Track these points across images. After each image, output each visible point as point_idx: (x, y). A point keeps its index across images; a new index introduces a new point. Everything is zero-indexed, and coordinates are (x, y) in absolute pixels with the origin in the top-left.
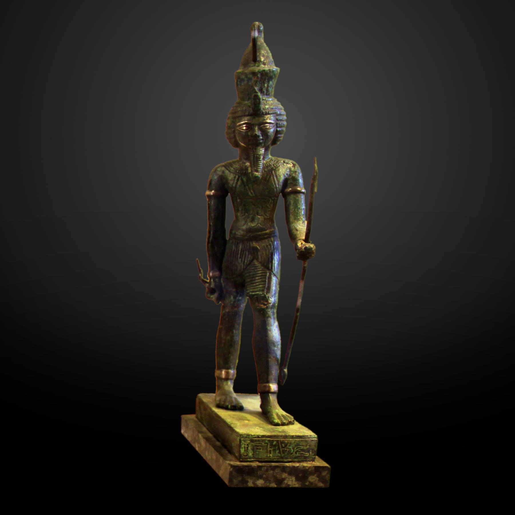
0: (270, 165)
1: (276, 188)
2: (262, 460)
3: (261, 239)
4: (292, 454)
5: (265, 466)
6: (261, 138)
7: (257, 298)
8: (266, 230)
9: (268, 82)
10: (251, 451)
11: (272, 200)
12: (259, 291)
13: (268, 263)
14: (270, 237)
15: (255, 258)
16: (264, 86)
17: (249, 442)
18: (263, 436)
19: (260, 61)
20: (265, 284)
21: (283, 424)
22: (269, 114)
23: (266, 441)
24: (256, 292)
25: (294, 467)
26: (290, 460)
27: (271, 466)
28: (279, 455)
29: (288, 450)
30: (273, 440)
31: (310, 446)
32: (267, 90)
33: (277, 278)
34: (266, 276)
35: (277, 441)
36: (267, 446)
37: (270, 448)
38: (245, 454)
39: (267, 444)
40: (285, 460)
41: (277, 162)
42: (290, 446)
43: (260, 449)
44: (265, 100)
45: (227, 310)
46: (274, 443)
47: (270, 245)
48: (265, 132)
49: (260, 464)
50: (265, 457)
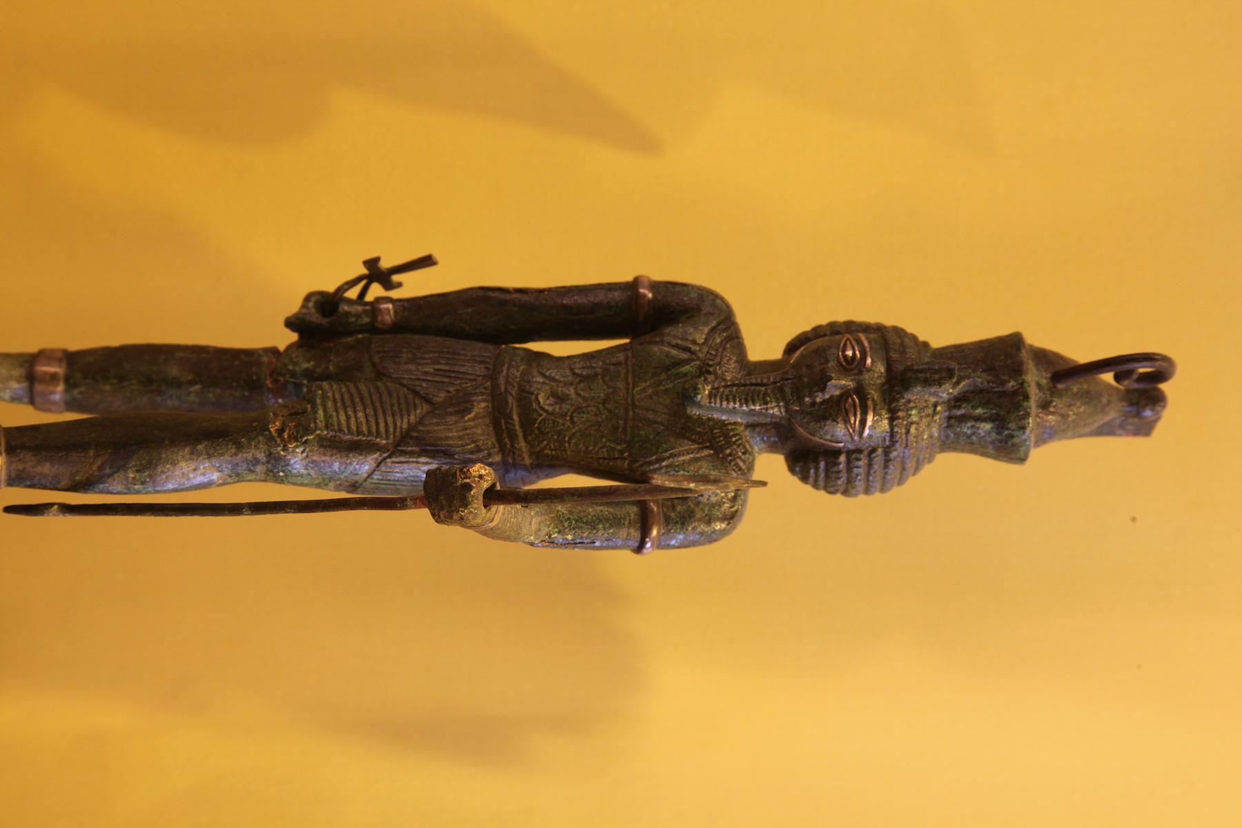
1: (659, 460)
3: (496, 425)
6: (818, 400)
7: (305, 411)
8: (526, 440)
9: (991, 419)
11: (622, 452)
12: (327, 416)
13: (419, 441)
14: (502, 450)
15: (437, 409)
16: (974, 408)
19: (1053, 391)
20: (350, 432)
22: (892, 420)
24: (324, 406)
32: (962, 419)
33: (370, 475)
34: (378, 434)
41: (740, 469)
44: (935, 413)
45: (265, 359)
47: (479, 450)
48: (836, 409)
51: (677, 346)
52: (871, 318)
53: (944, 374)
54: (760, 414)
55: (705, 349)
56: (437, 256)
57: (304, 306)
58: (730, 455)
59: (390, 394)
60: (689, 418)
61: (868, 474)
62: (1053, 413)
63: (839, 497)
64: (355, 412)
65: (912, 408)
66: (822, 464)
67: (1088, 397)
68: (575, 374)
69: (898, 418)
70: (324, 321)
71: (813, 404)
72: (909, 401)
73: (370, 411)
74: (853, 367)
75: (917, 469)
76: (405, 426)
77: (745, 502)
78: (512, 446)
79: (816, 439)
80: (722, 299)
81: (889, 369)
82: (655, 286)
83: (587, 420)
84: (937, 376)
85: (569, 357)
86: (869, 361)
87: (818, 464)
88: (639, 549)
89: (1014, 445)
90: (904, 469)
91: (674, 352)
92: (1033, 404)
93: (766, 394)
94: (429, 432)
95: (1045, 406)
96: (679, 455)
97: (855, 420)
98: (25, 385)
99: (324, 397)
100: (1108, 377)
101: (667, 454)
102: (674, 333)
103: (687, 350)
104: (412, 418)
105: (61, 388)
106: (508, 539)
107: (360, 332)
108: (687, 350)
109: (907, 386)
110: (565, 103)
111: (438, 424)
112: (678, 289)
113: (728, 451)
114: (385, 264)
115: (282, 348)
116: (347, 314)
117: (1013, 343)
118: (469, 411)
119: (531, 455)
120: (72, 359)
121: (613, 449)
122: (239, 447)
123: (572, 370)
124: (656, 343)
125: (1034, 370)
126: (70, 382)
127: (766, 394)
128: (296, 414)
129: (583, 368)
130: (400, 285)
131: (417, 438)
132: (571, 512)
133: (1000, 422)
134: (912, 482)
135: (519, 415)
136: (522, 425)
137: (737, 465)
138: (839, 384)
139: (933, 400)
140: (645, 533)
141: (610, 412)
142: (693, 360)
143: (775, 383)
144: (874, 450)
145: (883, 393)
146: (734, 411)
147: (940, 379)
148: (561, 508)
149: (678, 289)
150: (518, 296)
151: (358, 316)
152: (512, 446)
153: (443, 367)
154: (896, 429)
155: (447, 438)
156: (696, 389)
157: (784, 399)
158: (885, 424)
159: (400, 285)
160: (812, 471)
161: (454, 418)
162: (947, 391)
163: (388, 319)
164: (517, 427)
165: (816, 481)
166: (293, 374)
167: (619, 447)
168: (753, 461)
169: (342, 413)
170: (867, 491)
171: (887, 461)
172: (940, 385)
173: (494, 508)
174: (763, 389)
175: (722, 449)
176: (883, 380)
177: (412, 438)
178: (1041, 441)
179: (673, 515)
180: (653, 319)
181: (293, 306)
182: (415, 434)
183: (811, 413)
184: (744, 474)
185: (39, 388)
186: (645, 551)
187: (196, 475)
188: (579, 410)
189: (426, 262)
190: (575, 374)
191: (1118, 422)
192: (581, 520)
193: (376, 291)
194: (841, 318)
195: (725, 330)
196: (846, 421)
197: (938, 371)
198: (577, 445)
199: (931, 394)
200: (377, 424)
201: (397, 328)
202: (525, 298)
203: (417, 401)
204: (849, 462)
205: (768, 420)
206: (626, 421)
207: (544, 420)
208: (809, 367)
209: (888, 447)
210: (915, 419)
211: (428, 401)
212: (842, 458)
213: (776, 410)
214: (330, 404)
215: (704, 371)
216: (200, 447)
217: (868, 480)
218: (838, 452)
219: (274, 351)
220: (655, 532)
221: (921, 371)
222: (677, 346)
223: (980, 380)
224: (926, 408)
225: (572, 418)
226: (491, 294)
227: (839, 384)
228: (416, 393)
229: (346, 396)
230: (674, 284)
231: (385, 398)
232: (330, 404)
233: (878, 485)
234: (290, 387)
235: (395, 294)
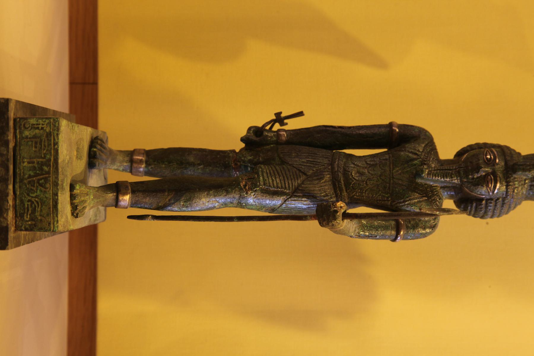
0: (433, 195)
1: (404, 202)
2: (18, 151)
3: (334, 185)
4: (28, 195)
5: (8, 152)
6: (475, 177)
10: (32, 134)
11: (388, 198)
17: (47, 130)
18: (57, 151)
20: (274, 187)
21: (73, 197)
22: (507, 186)
23: (48, 156)
24: (263, 175)
25: (7, 195)
26: (18, 193)
27: (8, 160)
28: (26, 176)
29: (35, 189)
30: (50, 165)
31: (41, 220)
34: (285, 188)
35: (48, 173)
36: (42, 158)
37: (38, 163)
38: (27, 126)
39: (45, 157)
40: (17, 186)
42: (41, 191)
43: (36, 147)
44: (525, 183)
46: (45, 168)
48: (483, 181)
49: (11, 145)
50: (22, 155)
51: (412, 152)
52: (495, 142)
53: (532, 167)
54: (449, 182)
55: (423, 154)
56: (304, 112)
58: (434, 200)
59: (289, 171)
60: (417, 183)
61: (494, 209)
64: (276, 178)
65: (516, 181)
66: (474, 205)
68: (367, 164)
69: (510, 185)
70: (257, 139)
71: (473, 178)
72: (515, 178)
73: (281, 178)
74: (490, 163)
75: (515, 208)
76: (296, 184)
77: (439, 220)
78: (341, 194)
79: (473, 194)
80: (428, 132)
82: (400, 126)
83: (373, 184)
84: (528, 168)
85: (363, 156)
86: (497, 161)
87: (473, 204)
88: (395, 240)
91: (410, 155)
93: (452, 174)
94: (306, 187)
96: (413, 199)
97: (491, 186)
98: (129, 164)
99: (262, 172)
101: (408, 199)
102: (409, 146)
103: (416, 154)
104: (299, 181)
107: (272, 144)
108: (416, 154)
109: (515, 171)
110: (346, 46)
111: (310, 184)
112: (409, 128)
113: (433, 198)
114: (283, 115)
115: (237, 151)
118: (322, 178)
119: (348, 198)
120: (148, 153)
121: (384, 196)
122: (228, 192)
123: (366, 162)
124: (403, 151)
126: (148, 164)
127: (452, 174)
128: (251, 178)
129: (371, 161)
130: (287, 124)
131: (302, 190)
132: (367, 224)
134: (512, 213)
135: (344, 181)
136: (345, 185)
137: (436, 204)
138: (485, 170)
139: (525, 178)
140: (398, 233)
141: (383, 180)
142: (418, 158)
143: (456, 169)
144: (498, 199)
147: (530, 168)
148: (364, 222)
149: (409, 128)
150: (340, 129)
151: (271, 137)
152: (341, 194)
153: (310, 160)
154: (509, 190)
155: (314, 190)
157: (460, 176)
159: (287, 124)
160: (469, 208)
161: (316, 182)
163: (284, 138)
164: (343, 186)
165: (470, 212)
166: (244, 162)
167: (387, 196)
169: (270, 179)
171: (503, 204)
172: (530, 171)
173: (345, 221)
174: (451, 171)
175: (430, 197)
177: (299, 190)
179: (409, 225)
180: (400, 141)
181: (244, 133)
182: (300, 188)
183: (472, 182)
185: (135, 165)
186: (397, 241)
187: (207, 203)
188: (369, 179)
189: (300, 114)
190: (367, 164)
192: (370, 227)
193: (277, 127)
194: (481, 141)
195: (431, 146)
196: (487, 186)
197: (529, 165)
198: (368, 194)
199: (524, 175)
200: (285, 184)
201: (288, 142)
203: (301, 174)
204: (486, 204)
205: (451, 185)
206: (390, 184)
207: (354, 183)
208: (471, 162)
209: (505, 198)
210: (517, 186)
211: (305, 174)
212: (484, 202)
213: (456, 181)
214: (265, 175)
216: (211, 192)
217: (494, 212)
218: (482, 200)
219: (234, 151)
220: (402, 233)
222: (412, 152)
224: (521, 182)
225: (366, 182)
226: (328, 128)
229: (271, 171)
230: (408, 126)
231: (288, 173)
232: (265, 175)
234: (242, 167)
235: (286, 128)
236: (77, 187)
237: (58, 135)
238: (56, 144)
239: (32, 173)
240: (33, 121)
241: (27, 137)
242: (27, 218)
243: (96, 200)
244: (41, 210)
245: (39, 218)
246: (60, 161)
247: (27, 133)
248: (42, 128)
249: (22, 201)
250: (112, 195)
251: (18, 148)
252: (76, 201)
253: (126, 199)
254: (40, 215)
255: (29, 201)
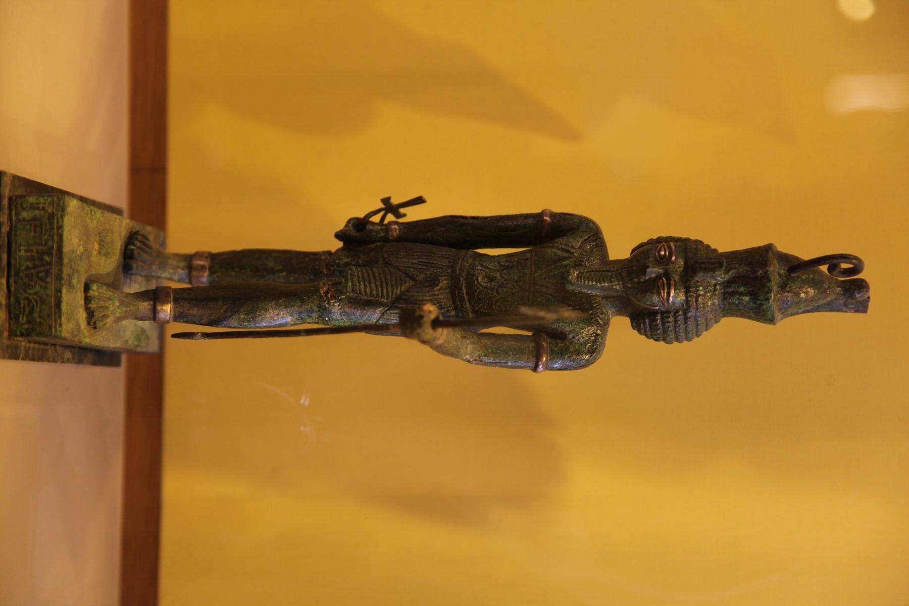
3: (453, 295)
6: (642, 280)
7: (341, 283)
14: (456, 309)
16: (739, 287)
18: (61, 237)
21: (88, 300)
22: (686, 293)
26: (13, 289)
28: (23, 268)
29: (32, 283)
32: (732, 294)
35: (50, 264)
37: (37, 252)
40: (12, 281)
42: (41, 286)
43: (35, 232)
44: (715, 290)
46: (47, 258)
48: (653, 286)
51: (562, 249)
54: (609, 289)
56: (425, 197)
57: (346, 226)
59: (391, 274)
61: (675, 327)
62: (789, 292)
63: (662, 343)
64: (370, 283)
66: (647, 321)
67: (816, 283)
70: (357, 234)
71: (639, 282)
73: (379, 283)
74: (664, 261)
76: (398, 292)
78: (462, 306)
79: (642, 304)
80: (594, 223)
81: (686, 263)
82: (553, 215)
86: (674, 258)
88: (535, 369)
89: (764, 310)
90: (698, 325)
91: (560, 253)
92: (774, 285)
93: (611, 277)
95: (783, 287)
98: (186, 271)
99: (352, 275)
100: (824, 268)
102: (561, 242)
104: (403, 288)
105: (206, 274)
106: (451, 355)
107: (379, 241)
108: (568, 251)
114: (395, 201)
116: (371, 230)
117: (768, 249)
119: (473, 312)
125: (777, 265)
126: (212, 271)
127: (611, 277)
128: (336, 284)
130: (405, 215)
133: (754, 296)
135: (466, 288)
136: (468, 294)
138: (653, 271)
139: (714, 282)
144: (677, 312)
145: (681, 277)
146: (592, 287)
148: (485, 341)
151: (378, 232)
156: (568, 272)
158: (682, 297)
159: (405, 215)
162: (721, 277)
163: (395, 234)
165: (645, 331)
166: (338, 266)
168: (609, 320)
169: (362, 283)
170: (678, 340)
171: (686, 319)
172: (714, 271)
176: (682, 269)
178: (787, 310)
181: (340, 225)
184: (601, 326)
185: (194, 273)
187: (280, 317)
188: (502, 285)
189: (419, 200)
191: (842, 302)
193: (390, 218)
196: (659, 294)
197: (714, 263)
200: (382, 290)
201: (400, 239)
202: (476, 221)
204: (662, 319)
205: (615, 294)
210: (701, 293)
211: (412, 278)
212: (659, 317)
214: (355, 279)
215: (578, 264)
216: (280, 301)
218: (655, 313)
221: (703, 263)
222: (562, 249)
223: (743, 269)
227: (653, 271)
228: (406, 274)
229: (365, 275)
231: (388, 277)
232: (355, 279)
233: (683, 334)
234: (337, 273)
235: (401, 220)
236: (95, 287)
237: (62, 216)
238: (60, 227)
239: (30, 264)
240: (32, 199)
241: (24, 219)
242: (23, 320)
243: (124, 309)
244: (41, 311)
245: (38, 320)
246: (65, 250)
247: (24, 214)
248: (43, 208)
249: (17, 300)
250: (146, 304)
251: (13, 233)
252: (93, 306)
253: (167, 310)
254: (40, 317)
255: (26, 299)
